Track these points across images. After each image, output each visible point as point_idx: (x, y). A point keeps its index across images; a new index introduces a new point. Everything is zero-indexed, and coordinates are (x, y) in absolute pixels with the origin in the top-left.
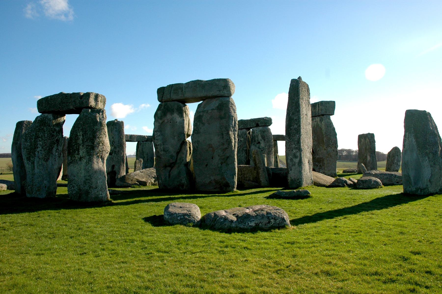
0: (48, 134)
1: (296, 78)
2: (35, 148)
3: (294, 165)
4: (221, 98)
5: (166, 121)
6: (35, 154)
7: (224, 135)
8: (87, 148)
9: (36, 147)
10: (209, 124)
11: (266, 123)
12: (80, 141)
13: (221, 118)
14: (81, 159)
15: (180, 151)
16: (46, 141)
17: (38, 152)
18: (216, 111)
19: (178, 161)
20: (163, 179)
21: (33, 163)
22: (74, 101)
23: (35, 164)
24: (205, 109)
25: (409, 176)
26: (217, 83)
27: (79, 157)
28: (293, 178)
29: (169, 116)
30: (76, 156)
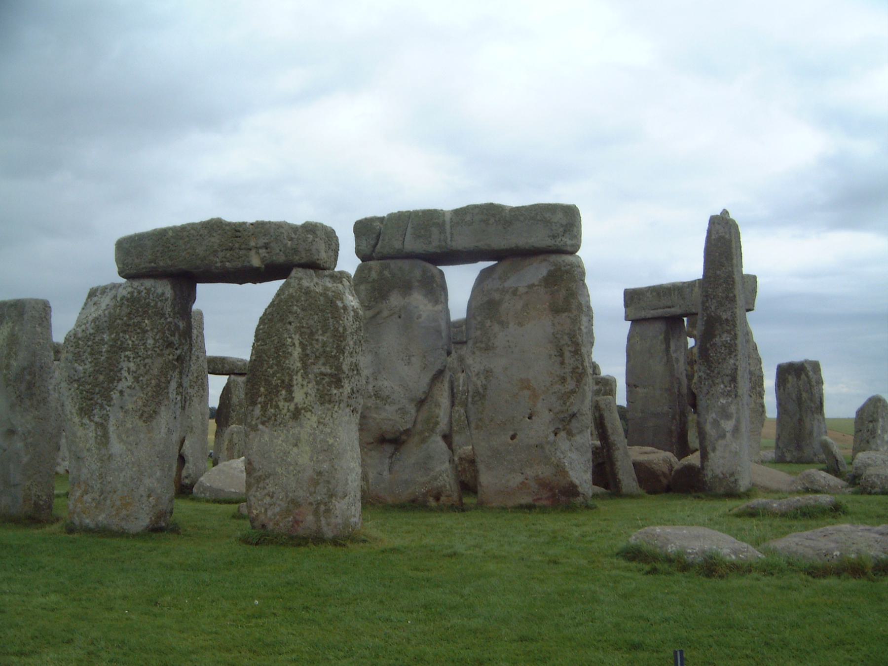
0: (156, 341)
1: (718, 212)
2: (112, 381)
4: (553, 258)
5: (385, 313)
6: (109, 399)
7: (567, 354)
8: (318, 383)
9: (113, 376)
10: (520, 324)
14: (296, 414)
15: (426, 398)
16: (147, 361)
17: (121, 392)
19: (419, 427)
22: (266, 246)
23: (111, 429)
26: (548, 215)
27: (292, 407)
28: (718, 472)
29: (395, 300)
30: (281, 404)
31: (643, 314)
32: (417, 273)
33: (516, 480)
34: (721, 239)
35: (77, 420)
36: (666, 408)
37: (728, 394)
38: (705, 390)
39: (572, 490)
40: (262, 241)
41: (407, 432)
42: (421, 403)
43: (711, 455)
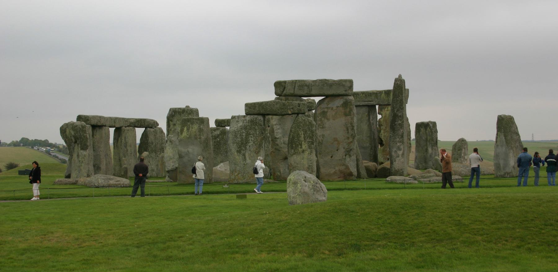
1: (397, 77)
3: (398, 157)
4: (345, 97)
6: (246, 148)
7: (350, 130)
9: (247, 142)
10: (334, 119)
11: (311, 107)
12: (302, 138)
13: (346, 115)
14: (303, 151)
18: (341, 108)
20: (282, 170)
21: (244, 155)
24: (329, 106)
25: (499, 164)
26: (344, 83)
31: (358, 104)
33: (332, 171)
35: (236, 154)
36: (368, 145)
37: (400, 142)
39: (351, 174)
40: (291, 107)
43: (394, 163)
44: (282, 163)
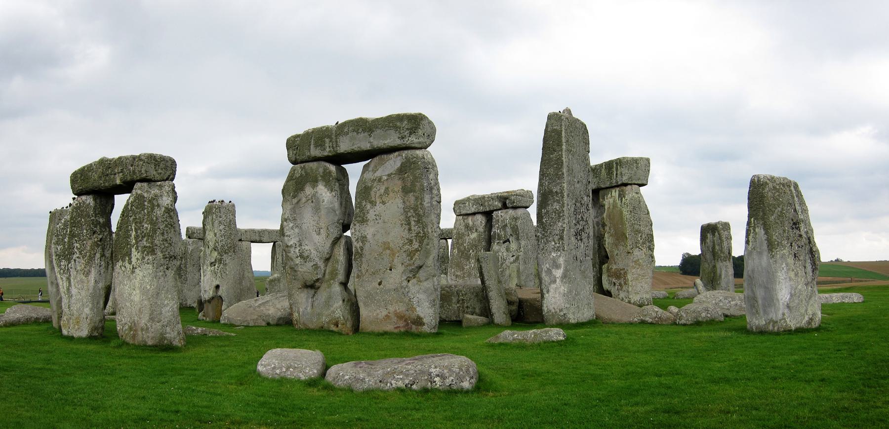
4: (405, 153)
5: (304, 200)
7: (413, 223)
10: (384, 203)
15: (330, 257)
19: (327, 277)
28: (551, 308)
29: (308, 190)
32: (321, 170)
34: (554, 131)
37: (558, 250)
38: (541, 246)
39: (419, 321)
41: (318, 280)
42: (327, 260)
43: (546, 295)
44: (302, 295)
